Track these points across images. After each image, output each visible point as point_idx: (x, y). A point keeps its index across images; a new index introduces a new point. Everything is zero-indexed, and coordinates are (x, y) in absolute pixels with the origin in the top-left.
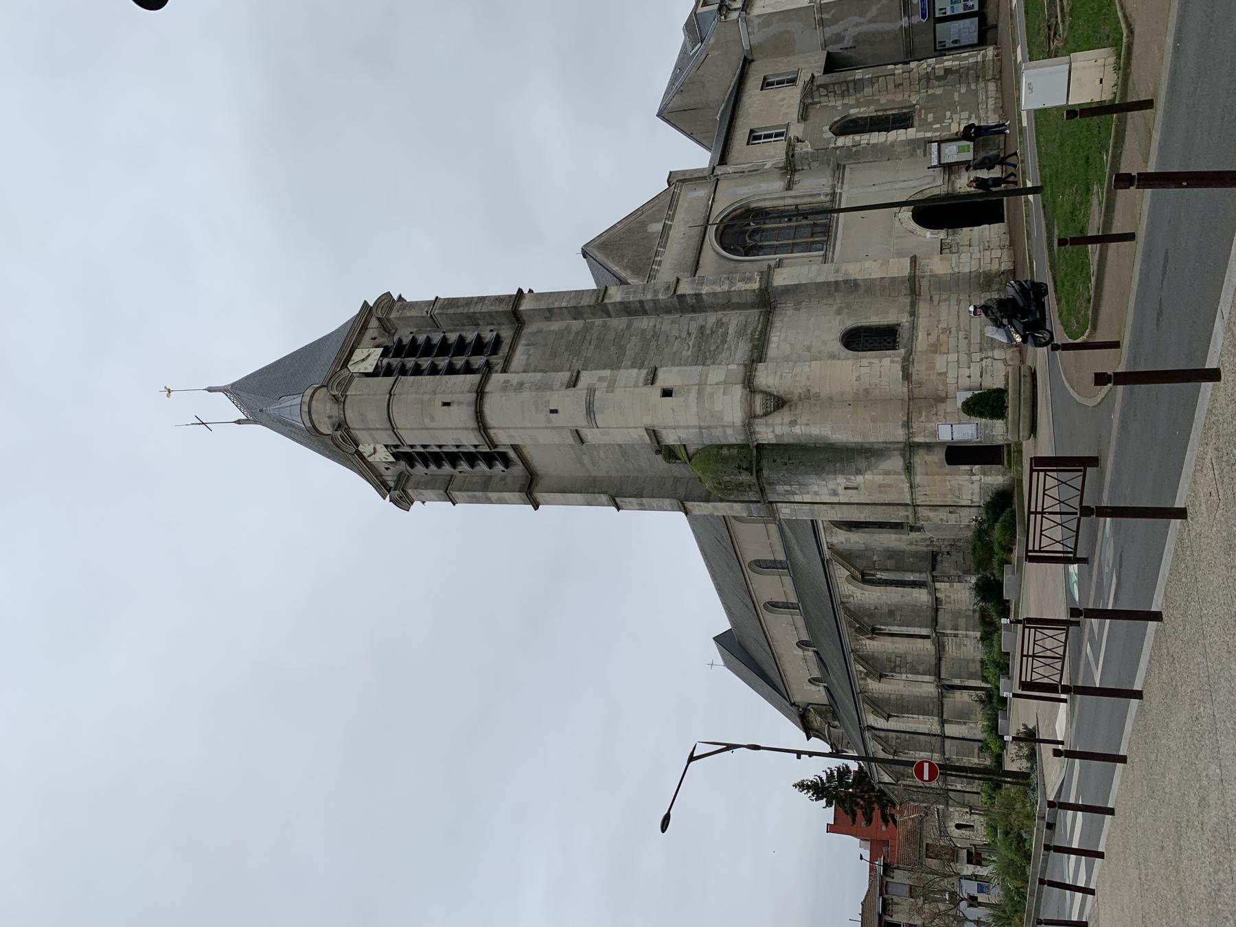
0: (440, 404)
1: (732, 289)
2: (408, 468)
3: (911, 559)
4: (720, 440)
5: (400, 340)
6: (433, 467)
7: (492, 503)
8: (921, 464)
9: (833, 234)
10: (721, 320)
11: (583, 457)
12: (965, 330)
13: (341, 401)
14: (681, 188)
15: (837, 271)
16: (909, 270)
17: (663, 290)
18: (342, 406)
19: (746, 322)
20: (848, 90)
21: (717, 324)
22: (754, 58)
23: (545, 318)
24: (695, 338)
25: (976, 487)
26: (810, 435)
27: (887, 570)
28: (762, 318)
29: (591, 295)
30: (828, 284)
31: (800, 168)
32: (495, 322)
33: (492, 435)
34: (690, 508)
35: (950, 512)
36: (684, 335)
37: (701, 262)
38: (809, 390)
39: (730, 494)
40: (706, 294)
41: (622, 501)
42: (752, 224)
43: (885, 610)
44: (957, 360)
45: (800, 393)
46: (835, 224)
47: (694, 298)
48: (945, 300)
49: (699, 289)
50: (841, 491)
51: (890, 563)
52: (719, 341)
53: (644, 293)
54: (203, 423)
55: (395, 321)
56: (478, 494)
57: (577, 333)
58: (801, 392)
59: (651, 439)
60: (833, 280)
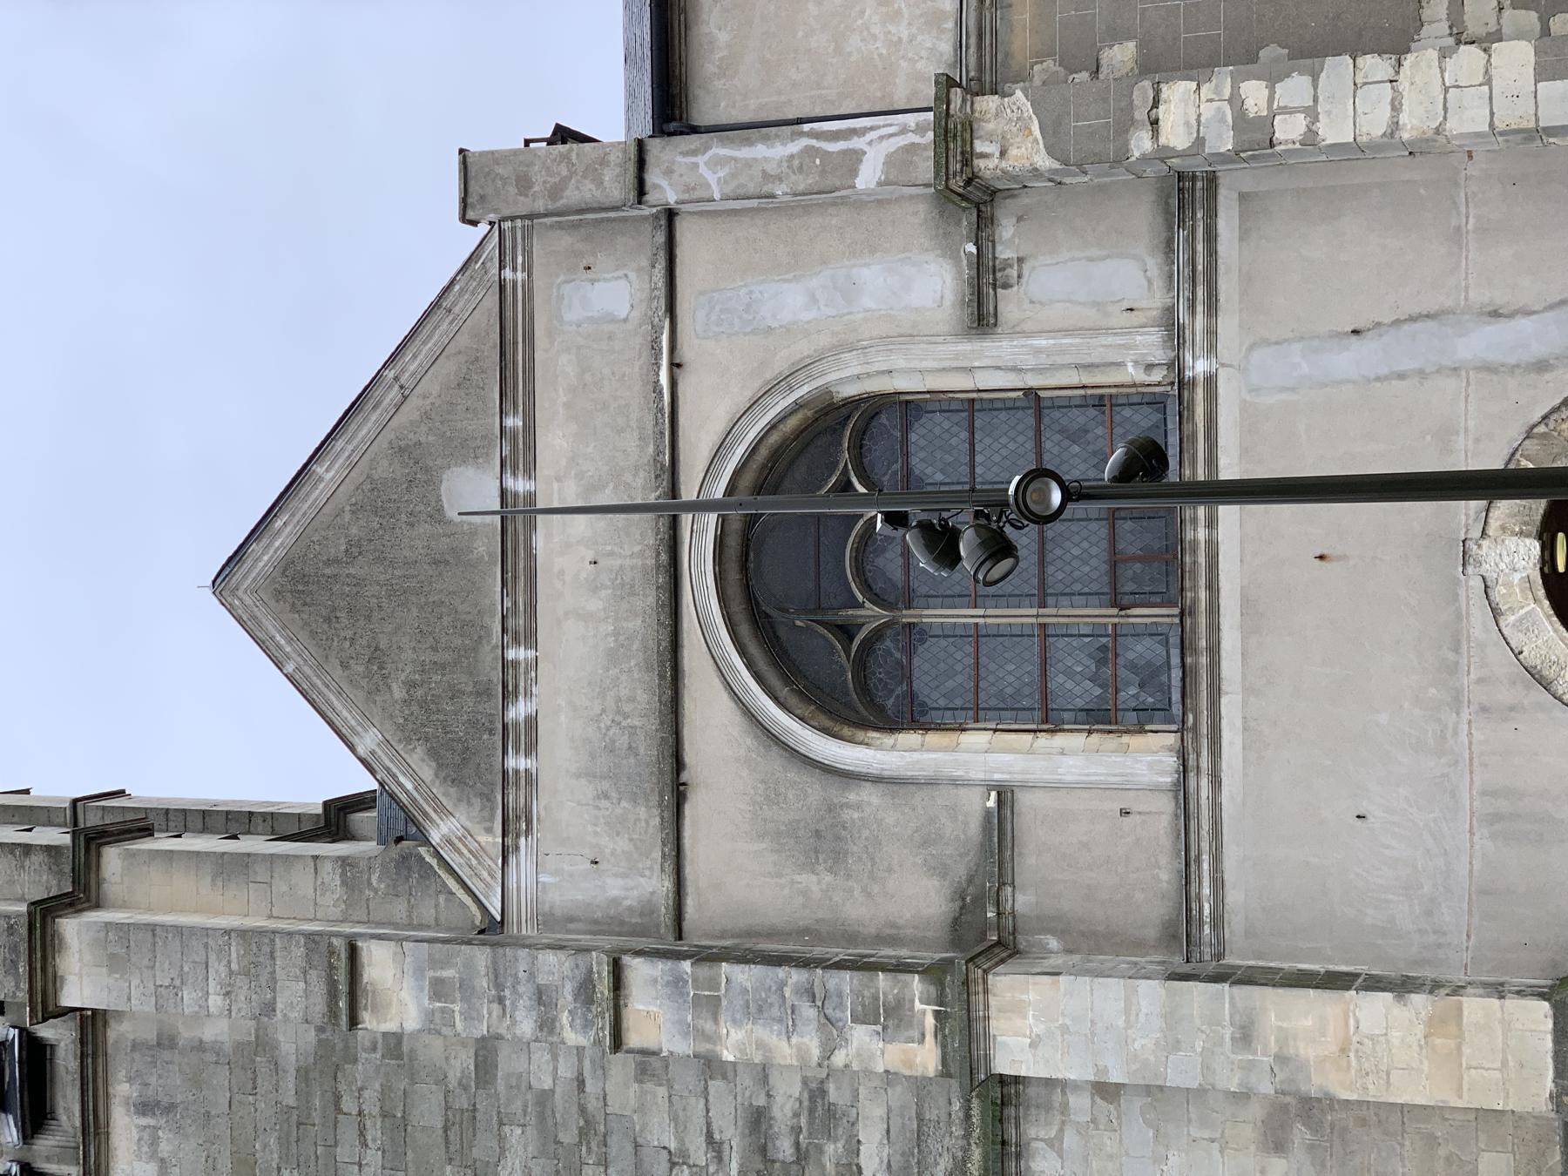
9: (1203, 660)
10: (823, 1093)
14: (528, 254)
16: (1549, 1084)
19: (920, 1118)
21: (812, 1111)
28: (975, 1103)
29: (305, 973)
37: (689, 756)
46: (1203, 595)
53: (501, 1000)
57: (303, 1074)
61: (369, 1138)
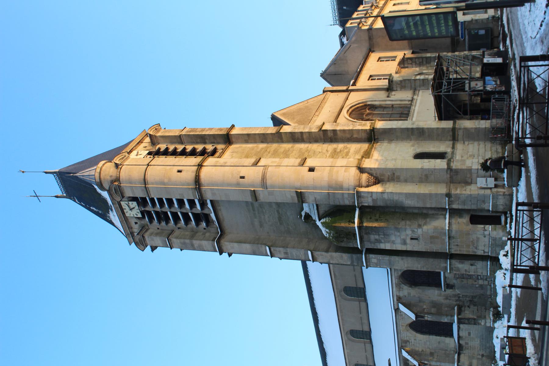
0: (176, 171)
1: (354, 129)
2: (149, 223)
3: (446, 309)
4: (339, 202)
5: (159, 149)
6: (163, 223)
7: (194, 249)
8: (455, 223)
11: (255, 219)
12: (482, 156)
13: (119, 168)
15: (413, 124)
17: (315, 128)
18: (119, 170)
20: (423, 62)
22: (375, 50)
23: (245, 140)
24: (331, 153)
25: (486, 239)
26: (393, 201)
27: (431, 313)
30: (407, 129)
31: (396, 89)
32: (215, 142)
33: (203, 192)
34: (317, 256)
35: (472, 265)
36: (324, 151)
38: (394, 174)
39: (342, 242)
40: (340, 130)
41: (274, 250)
42: (367, 111)
43: (428, 351)
44: (477, 161)
45: (389, 175)
47: (332, 132)
48: (472, 144)
49: (335, 128)
50: (408, 241)
51: (433, 310)
52: (344, 155)
54: (37, 196)
55: (159, 138)
56: (187, 241)
58: (390, 174)
59: (298, 200)
60: (411, 127)
61: (270, 153)
